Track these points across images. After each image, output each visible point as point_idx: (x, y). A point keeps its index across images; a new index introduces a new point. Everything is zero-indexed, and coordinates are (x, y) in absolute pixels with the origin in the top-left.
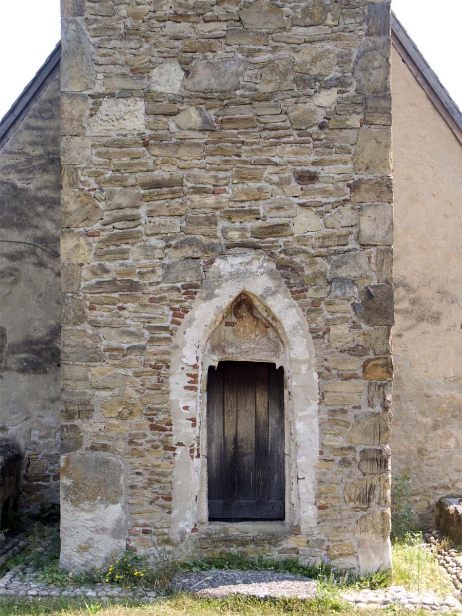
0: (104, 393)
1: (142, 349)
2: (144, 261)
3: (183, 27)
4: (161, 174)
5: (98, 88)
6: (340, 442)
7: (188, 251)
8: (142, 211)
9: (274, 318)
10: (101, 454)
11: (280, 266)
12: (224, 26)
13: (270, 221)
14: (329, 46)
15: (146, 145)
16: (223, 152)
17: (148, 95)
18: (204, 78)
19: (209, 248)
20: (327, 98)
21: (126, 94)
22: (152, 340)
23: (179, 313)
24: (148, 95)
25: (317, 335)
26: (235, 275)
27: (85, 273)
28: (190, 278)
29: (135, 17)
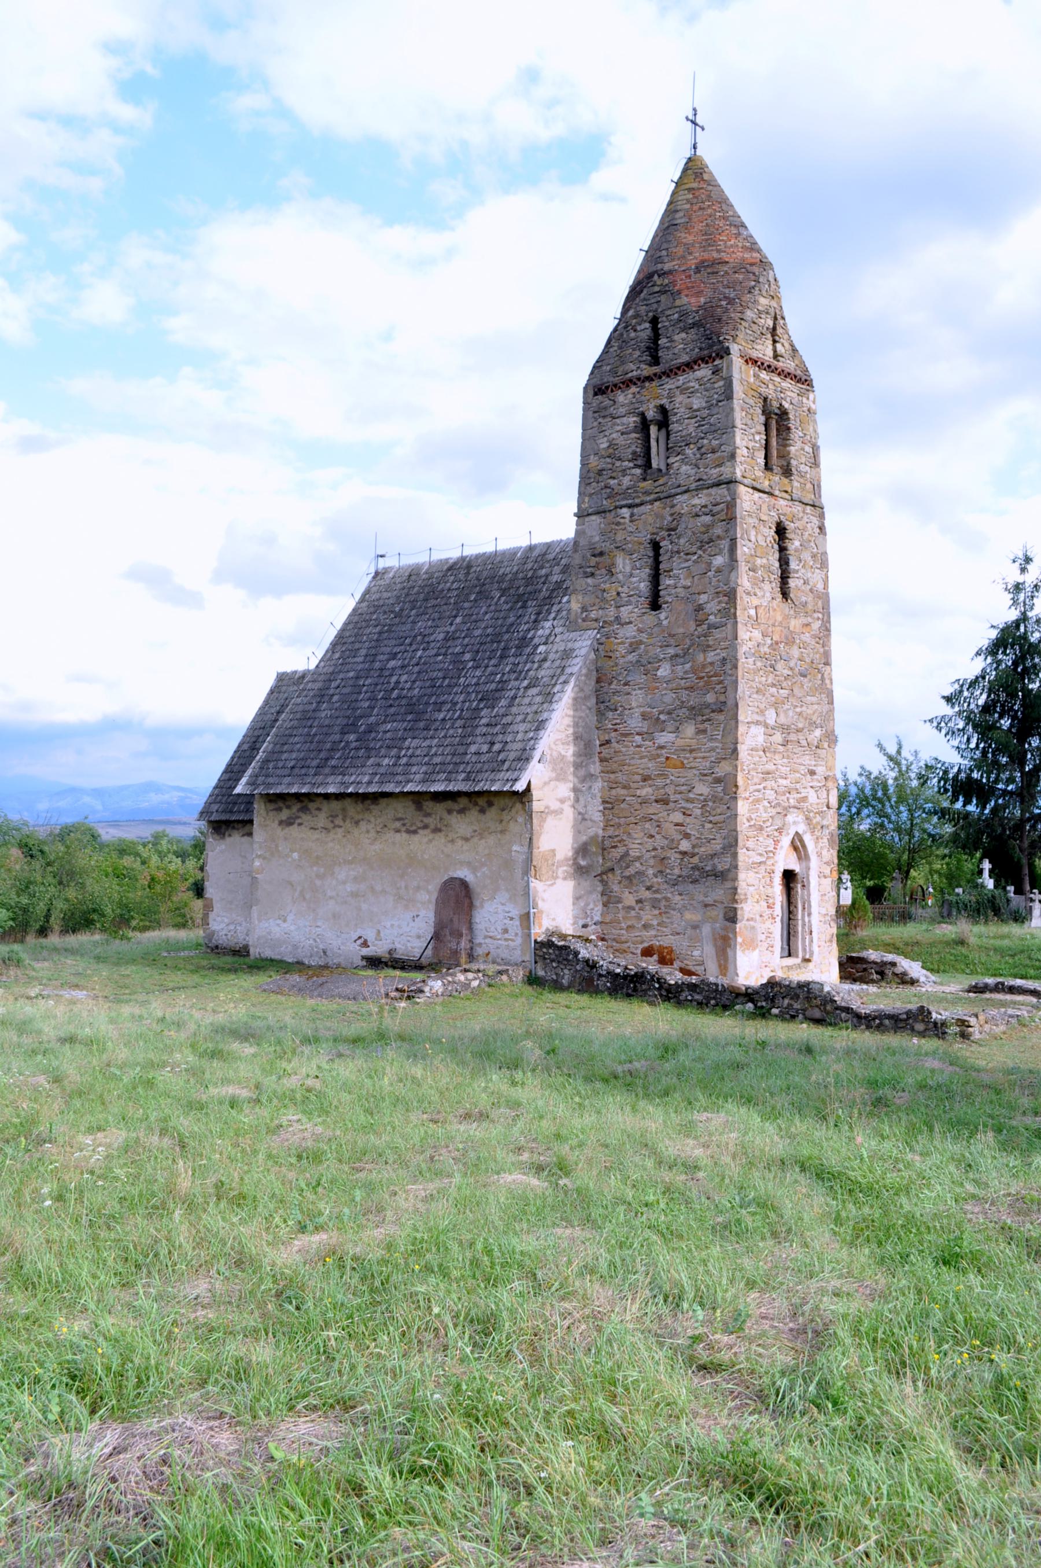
0: (751, 889)
1: (764, 863)
2: (764, 815)
3: (774, 690)
4: (770, 767)
5: (749, 720)
6: (824, 911)
7: (779, 810)
8: (761, 787)
9: (804, 846)
10: (752, 923)
11: (807, 819)
12: (786, 692)
13: (803, 795)
14: (816, 707)
15: (764, 751)
16: (788, 757)
17: (766, 726)
18: (782, 720)
19: (785, 809)
20: (818, 733)
21: (758, 723)
22: (768, 858)
23: (776, 842)
24: (766, 726)
25: (819, 855)
26: (795, 823)
27: (745, 821)
28: (778, 823)
29: (760, 683)
